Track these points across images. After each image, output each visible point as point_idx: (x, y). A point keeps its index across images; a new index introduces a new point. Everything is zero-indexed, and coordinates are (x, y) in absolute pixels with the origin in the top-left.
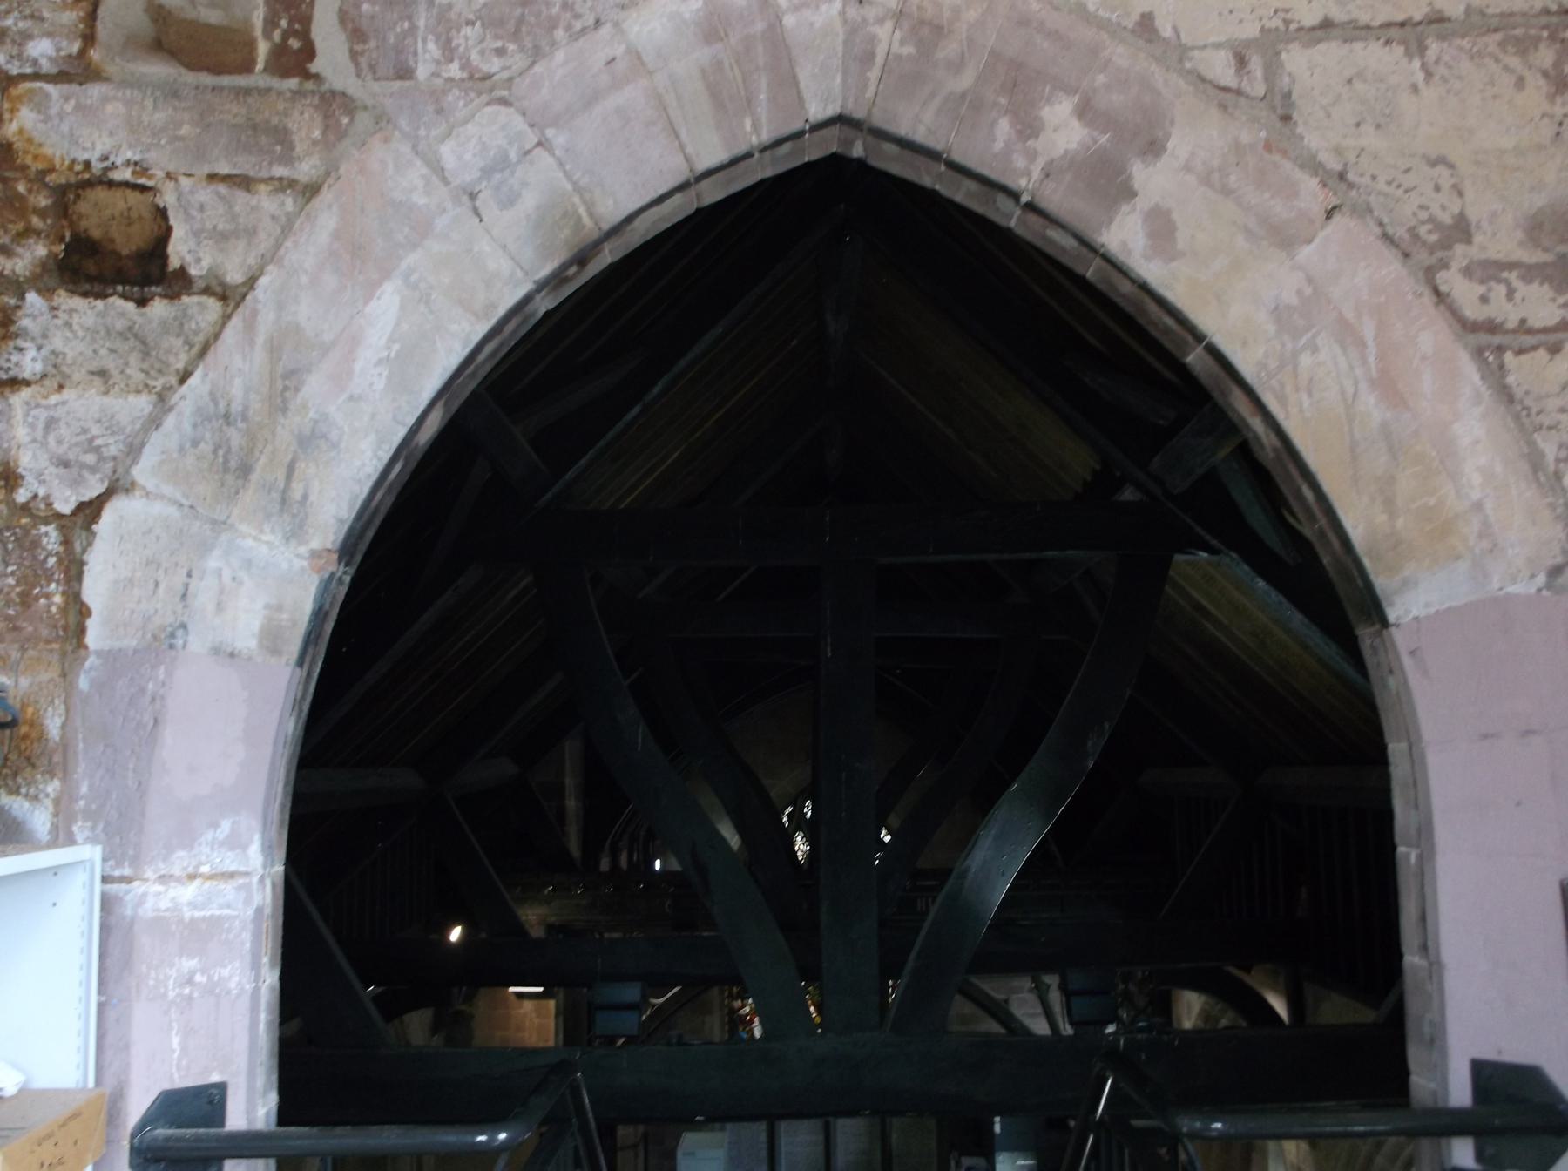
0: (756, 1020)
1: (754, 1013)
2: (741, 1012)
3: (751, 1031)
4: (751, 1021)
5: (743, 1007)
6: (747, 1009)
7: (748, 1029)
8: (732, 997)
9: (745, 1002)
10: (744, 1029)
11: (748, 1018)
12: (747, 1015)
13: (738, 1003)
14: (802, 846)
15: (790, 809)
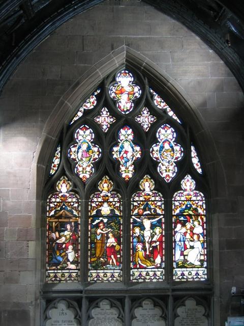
0: (70, 247)
1: (69, 243)
2: (58, 241)
3: (67, 255)
4: (67, 248)
5: (60, 237)
6: (63, 239)
7: (63, 254)
8: (51, 229)
9: (62, 234)
10: (60, 254)
11: (64, 246)
12: (64, 243)
13: (55, 235)
14: (106, 118)
15: (99, 91)
